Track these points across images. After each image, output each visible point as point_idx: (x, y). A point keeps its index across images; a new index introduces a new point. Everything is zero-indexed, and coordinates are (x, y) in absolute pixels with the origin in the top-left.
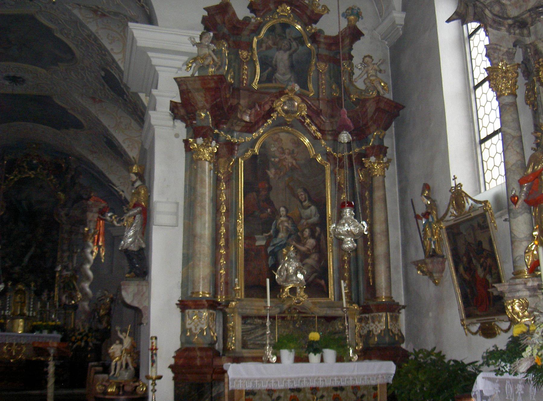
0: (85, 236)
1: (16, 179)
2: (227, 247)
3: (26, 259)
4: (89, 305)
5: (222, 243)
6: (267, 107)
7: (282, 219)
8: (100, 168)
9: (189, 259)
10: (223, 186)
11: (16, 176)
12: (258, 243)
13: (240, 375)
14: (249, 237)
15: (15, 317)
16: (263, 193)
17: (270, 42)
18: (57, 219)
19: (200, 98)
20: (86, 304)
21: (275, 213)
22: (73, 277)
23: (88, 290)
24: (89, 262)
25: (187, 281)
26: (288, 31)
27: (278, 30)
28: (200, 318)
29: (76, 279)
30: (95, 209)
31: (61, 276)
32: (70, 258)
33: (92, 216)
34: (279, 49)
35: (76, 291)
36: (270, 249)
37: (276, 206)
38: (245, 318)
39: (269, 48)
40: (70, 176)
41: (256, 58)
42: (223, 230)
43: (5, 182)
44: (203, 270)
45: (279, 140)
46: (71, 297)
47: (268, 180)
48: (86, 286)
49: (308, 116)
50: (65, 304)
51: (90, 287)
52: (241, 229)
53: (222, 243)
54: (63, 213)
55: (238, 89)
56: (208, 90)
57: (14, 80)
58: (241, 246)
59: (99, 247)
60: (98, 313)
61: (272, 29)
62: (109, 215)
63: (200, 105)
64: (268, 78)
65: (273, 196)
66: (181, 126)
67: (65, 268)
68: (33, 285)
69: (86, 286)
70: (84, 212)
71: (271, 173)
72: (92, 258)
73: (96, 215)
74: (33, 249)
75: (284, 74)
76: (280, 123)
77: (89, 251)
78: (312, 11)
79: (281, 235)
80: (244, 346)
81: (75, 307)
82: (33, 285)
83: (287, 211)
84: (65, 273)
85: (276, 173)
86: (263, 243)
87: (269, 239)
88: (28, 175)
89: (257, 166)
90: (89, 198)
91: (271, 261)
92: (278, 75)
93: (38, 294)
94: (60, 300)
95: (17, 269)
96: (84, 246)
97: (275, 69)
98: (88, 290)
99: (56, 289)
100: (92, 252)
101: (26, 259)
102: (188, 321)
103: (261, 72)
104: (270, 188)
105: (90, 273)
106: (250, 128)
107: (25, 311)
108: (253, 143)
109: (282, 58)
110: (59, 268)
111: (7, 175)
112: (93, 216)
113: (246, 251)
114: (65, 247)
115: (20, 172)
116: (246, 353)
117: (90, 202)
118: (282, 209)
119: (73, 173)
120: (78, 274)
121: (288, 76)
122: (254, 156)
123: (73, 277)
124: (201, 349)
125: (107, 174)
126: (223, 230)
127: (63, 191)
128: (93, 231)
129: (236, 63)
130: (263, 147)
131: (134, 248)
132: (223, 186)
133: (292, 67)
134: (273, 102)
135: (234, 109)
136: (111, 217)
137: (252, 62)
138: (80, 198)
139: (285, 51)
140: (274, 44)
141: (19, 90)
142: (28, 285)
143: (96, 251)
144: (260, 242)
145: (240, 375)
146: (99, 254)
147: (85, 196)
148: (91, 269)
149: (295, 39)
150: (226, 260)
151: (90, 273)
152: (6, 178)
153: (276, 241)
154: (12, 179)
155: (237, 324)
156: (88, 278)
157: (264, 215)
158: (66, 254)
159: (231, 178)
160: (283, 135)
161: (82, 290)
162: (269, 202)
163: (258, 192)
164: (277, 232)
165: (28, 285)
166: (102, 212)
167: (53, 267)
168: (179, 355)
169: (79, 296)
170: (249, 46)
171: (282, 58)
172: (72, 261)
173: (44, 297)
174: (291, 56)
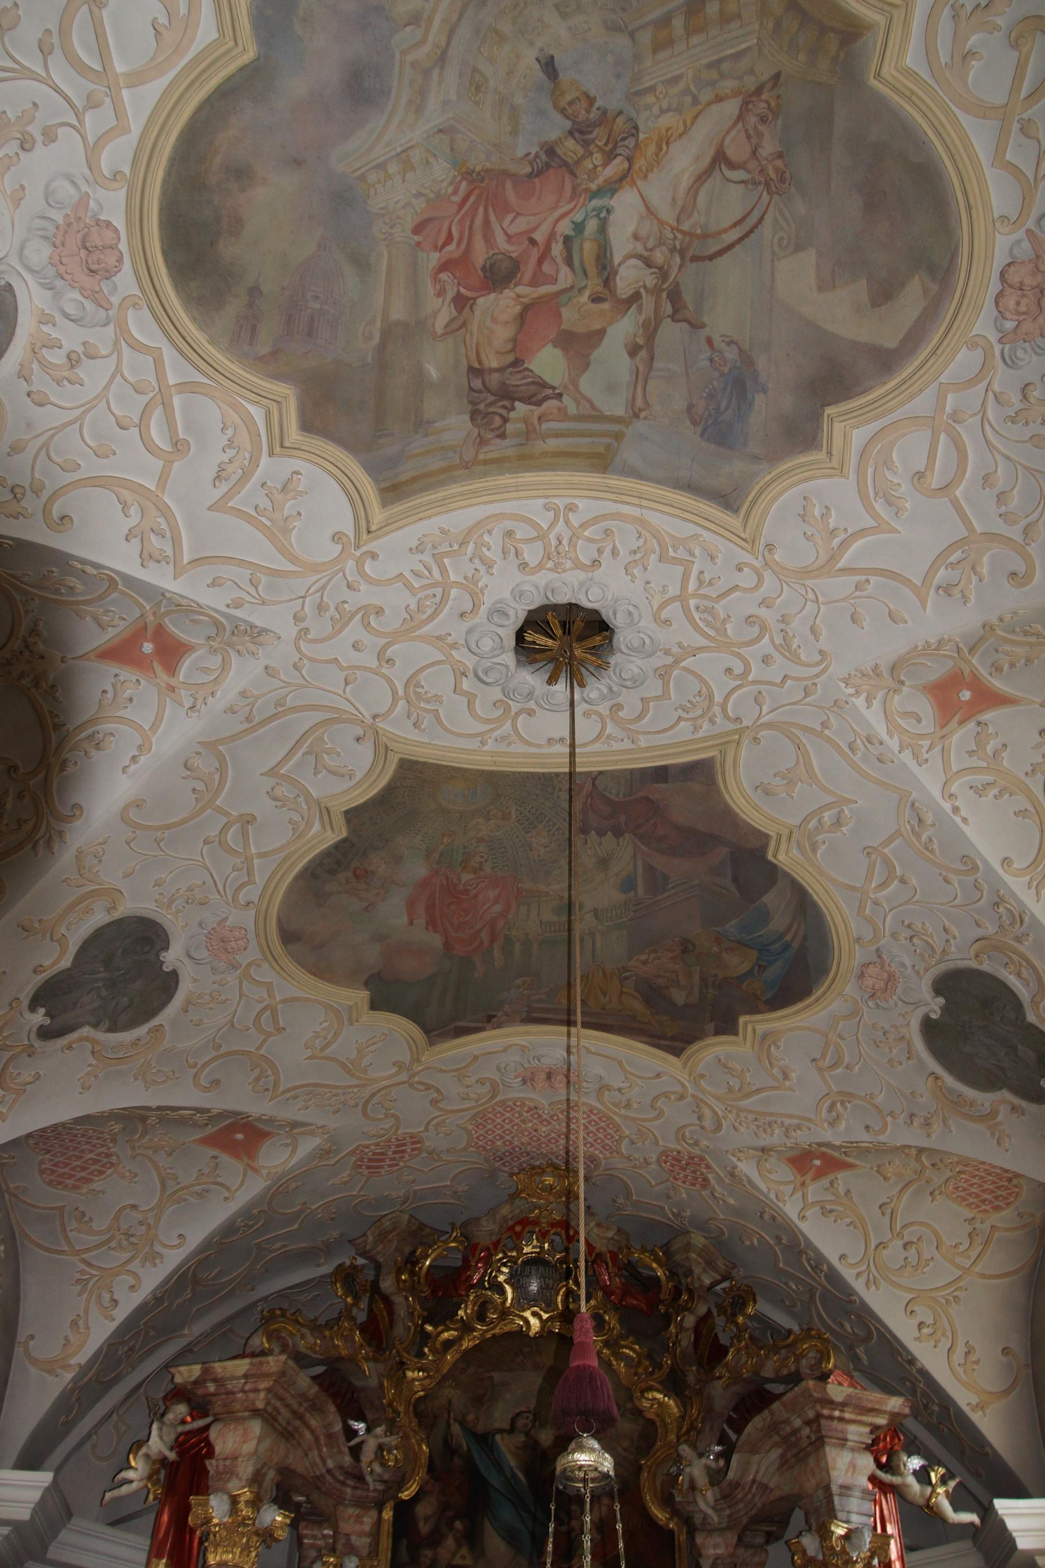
1: (466, 1344)
8: (832, 1256)
11: (466, 1328)
18: (660, 1515)
30: (858, 1433)
33: (849, 1467)
40: (690, 1321)
43: (421, 1355)
54: (697, 1470)
57: (566, 638)
62: (915, 1463)
70: (806, 1447)
73: (867, 1463)
88: (513, 1327)
111: (429, 1328)
112: (853, 1466)
115: (481, 1317)
117: (837, 1390)
119: (702, 1310)
125: (859, 1286)
127: (674, 1385)
136: (922, 1475)
138: (755, 1399)
152: (425, 1337)
154: (448, 1344)
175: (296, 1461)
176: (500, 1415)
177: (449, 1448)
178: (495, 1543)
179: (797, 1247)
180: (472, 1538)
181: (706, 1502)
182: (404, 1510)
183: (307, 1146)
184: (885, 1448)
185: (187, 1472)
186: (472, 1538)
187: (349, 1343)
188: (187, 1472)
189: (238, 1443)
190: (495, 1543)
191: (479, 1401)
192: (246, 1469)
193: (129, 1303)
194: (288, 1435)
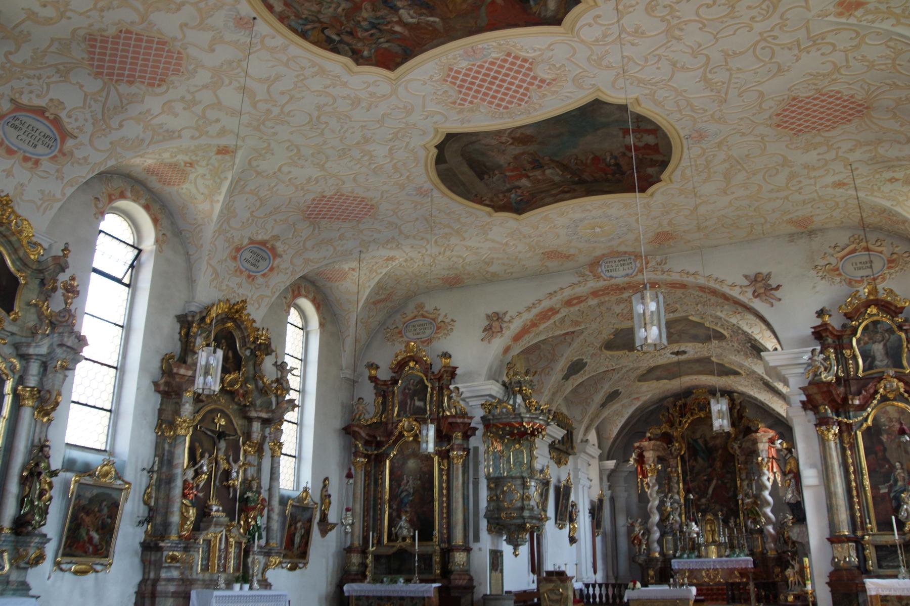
0: (759, 465)
2: (858, 496)
3: (710, 491)
4: (774, 529)
5: (854, 493)
6: (872, 391)
7: (899, 471)
8: (763, 400)
9: (831, 509)
10: (849, 452)
12: (882, 491)
13: (875, 586)
14: (873, 487)
15: (707, 545)
16: (880, 454)
17: (866, 339)
19: (819, 398)
20: (770, 528)
21: (892, 468)
22: (755, 503)
23: (770, 514)
24: (766, 488)
25: (832, 525)
26: (879, 326)
27: (871, 328)
28: (842, 549)
29: (757, 505)
30: (765, 439)
31: (743, 503)
32: (750, 486)
33: (763, 446)
34: (874, 342)
35: (759, 516)
36: (892, 495)
37: (892, 462)
38: (878, 548)
39: (865, 343)
41: (858, 353)
42: (854, 484)
44: (843, 516)
45: (886, 412)
46: (756, 521)
47: (881, 442)
48: (768, 510)
49: (905, 391)
50: (751, 529)
51: (772, 511)
52: (867, 482)
53: (854, 493)
54: (736, 446)
55: (848, 380)
56: (823, 393)
57: (677, 353)
58: (869, 494)
59: (774, 473)
60: (783, 536)
61: (866, 328)
62: (780, 441)
63: (820, 402)
64: (869, 366)
65: (888, 455)
66: (811, 414)
67: (747, 495)
68: (720, 514)
69: (768, 510)
70: (755, 442)
71: (884, 438)
72: (769, 485)
74: (714, 482)
75: (881, 361)
76: (884, 399)
77: (765, 478)
78: (896, 307)
79: (900, 483)
80: (880, 567)
81: (761, 531)
82: (720, 514)
83: (902, 465)
84: (748, 501)
85: (888, 437)
86: (886, 491)
87: (890, 488)
89: (872, 434)
90: (756, 431)
91: (894, 503)
92: (877, 363)
93: (726, 522)
94: (746, 526)
95: (703, 500)
96: (761, 474)
97: (874, 359)
98: (770, 514)
99: (741, 515)
100: (769, 479)
101: (710, 491)
102: (835, 552)
103: (864, 363)
104: (885, 450)
105: (770, 499)
106: (862, 407)
107: (717, 539)
108: (866, 419)
109: (878, 349)
110: (740, 497)
113: (874, 498)
114: (744, 476)
116: (882, 572)
118: (897, 464)
120: (758, 500)
121: (885, 362)
122: (869, 428)
123: (755, 503)
124: (846, 570)
126: (854, 484)
128: (766, 460)
129: (841, 360)
130: (874, 419)
131: (792, 501)
132: (849, 452)
133: (887, 354)
134: (875, 386)
135: (845, 400)
137: (854, 357)
139: (880, 342)
140: (870, 339)
141: (682, 357)
142: (716, 515)
143: (772, 478)
144: (884, 490)
145: (875, 586)
146: (775, 481)
147: (753, 429)
148: (770, 494)
149: (887, 331)
150: (859, 505)
151: (770, 499)
153: (897, 488)
155: (870, 552)
156: (768, 504)
157: (883, 470)
158: (746, 483)
159: (854, 446)
160: (888, 408)
161: (765, 515)
162: (888, 461)
163: (876, 454)
164: (896, 481)
165: (716, 515)
166: (772, 441)
167: (736, 496)
168: (831, 575)
169: (763, 520)
170: (851, 347)
171: (878, 349)
172: (752, 489)
173: (732, 524)
174: (885, 345)
175: (660, 454)
176: (698, 435)
177: (689, 444)
178: (700, 460)
179: (756, 399)
180: (695, 460)
181: (738, 452)
182: (682, 458)
183: (648, 396)
184: (772, 441)
185: (641, 460)
186: (695, 460)
187: (665, 428)
188: (641, 460)
189: (649, 455)
190: (700, 460)
191: (694, 433)
192: (651, 460)
193: (620, 425)
194: (658, 450)
